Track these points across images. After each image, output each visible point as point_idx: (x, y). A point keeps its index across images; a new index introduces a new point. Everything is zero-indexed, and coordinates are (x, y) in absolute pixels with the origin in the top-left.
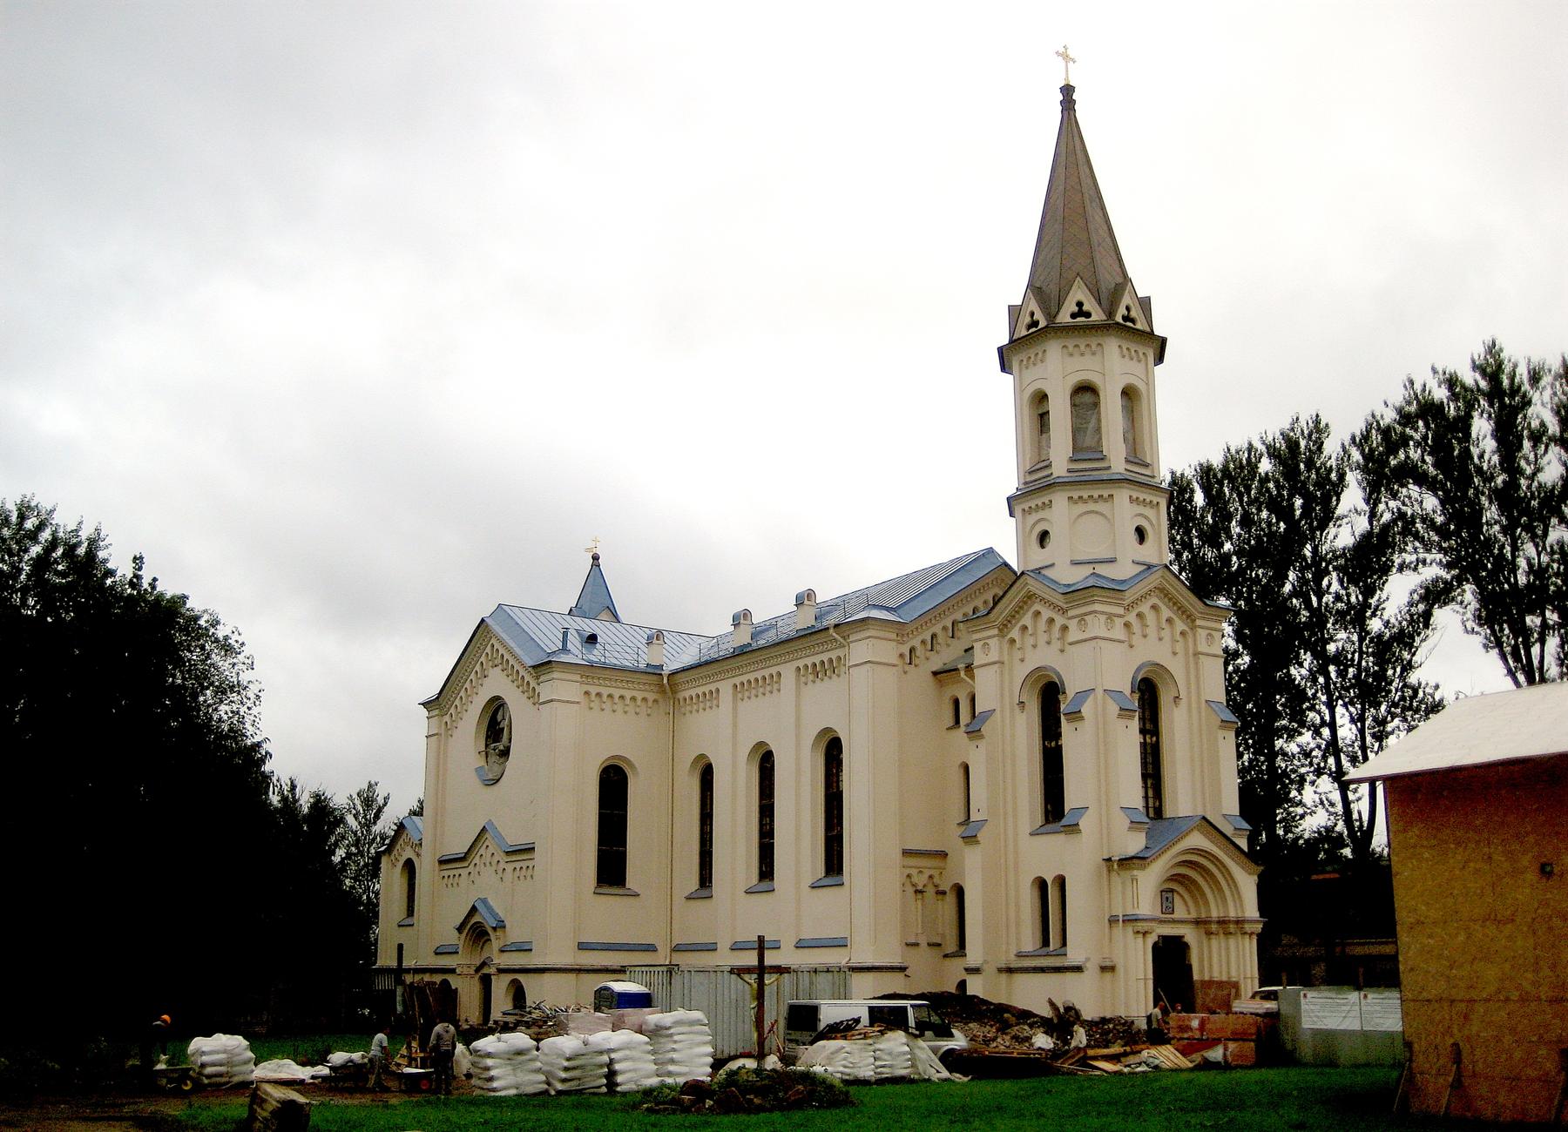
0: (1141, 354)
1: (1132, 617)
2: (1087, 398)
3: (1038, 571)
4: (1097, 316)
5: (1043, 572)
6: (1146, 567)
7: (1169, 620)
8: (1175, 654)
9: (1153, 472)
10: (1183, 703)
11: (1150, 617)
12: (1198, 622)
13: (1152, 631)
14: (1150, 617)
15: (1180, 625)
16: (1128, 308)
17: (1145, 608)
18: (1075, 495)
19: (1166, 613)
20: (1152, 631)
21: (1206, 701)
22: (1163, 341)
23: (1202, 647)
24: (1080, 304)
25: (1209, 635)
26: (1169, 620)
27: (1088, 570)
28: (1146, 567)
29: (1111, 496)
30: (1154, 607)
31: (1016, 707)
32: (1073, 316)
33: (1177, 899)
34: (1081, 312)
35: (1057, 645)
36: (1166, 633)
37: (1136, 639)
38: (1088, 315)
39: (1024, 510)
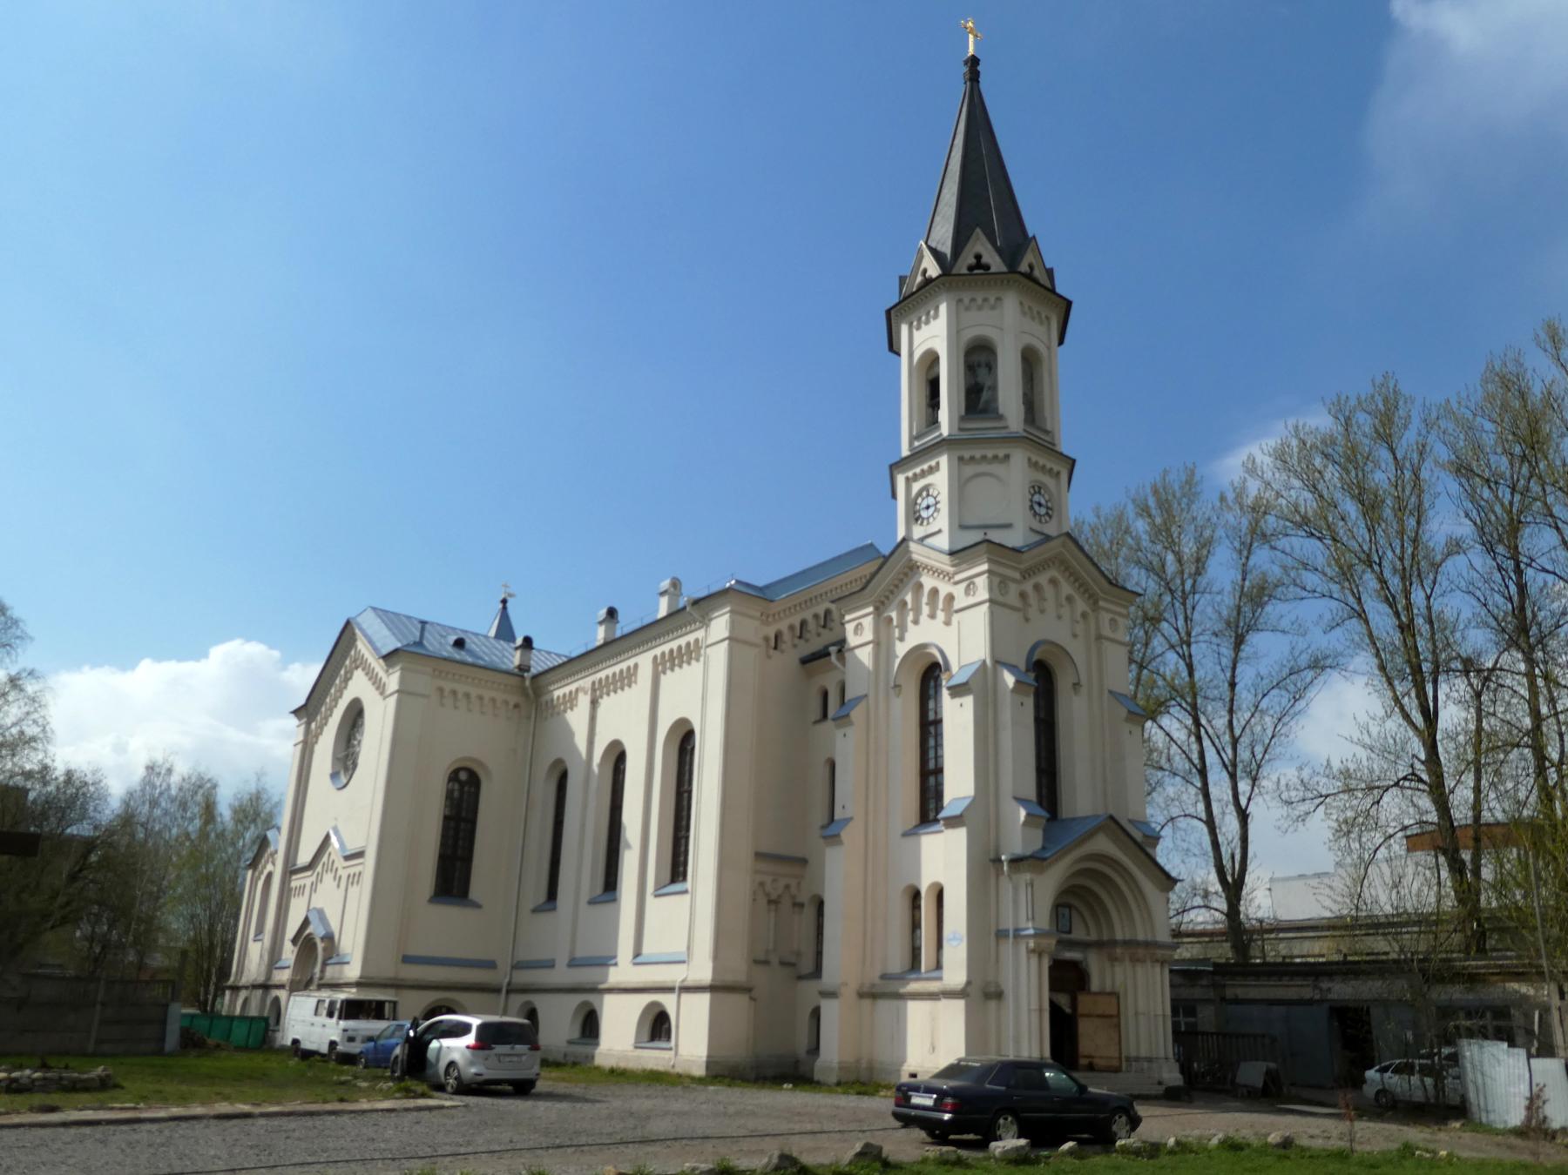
0: (1043, 316)
1: (1028, 587)
2: (982, 358)
3: (922, 540)
4: (996, 263)
5: (929, 541)
6: (1042, 537)
7: (1069, 599)
8: (1075, 636)
9: (1053, 438)
10: (1084, 690)
11: (1049, 591)
12: (1101, 603)
13: (1050, 605)
14: (1049, 591)
15: (1081, 605)
16: (1031, 267)
17: (1043, 579)
18: (967, 455)
19: (1066, 589)
20: (1050, 605)
21: (1111, 692)
22: (1069, 303)
23: (1106, 631)
24: (978, 257)
25: (1112, 620)
26: (1069, 599)
27: (976, 536)
28: (1042, 537)
29: (1007, 457)
30: (1053, 581)
31: (892, 692)
32: (971, 268)
33: (1076, 920)
34: (979, 264)
35: (941, 615)
36: (1065, 612)
37: (1033, 612)
38: (987, 267)
39: (907, 479)
